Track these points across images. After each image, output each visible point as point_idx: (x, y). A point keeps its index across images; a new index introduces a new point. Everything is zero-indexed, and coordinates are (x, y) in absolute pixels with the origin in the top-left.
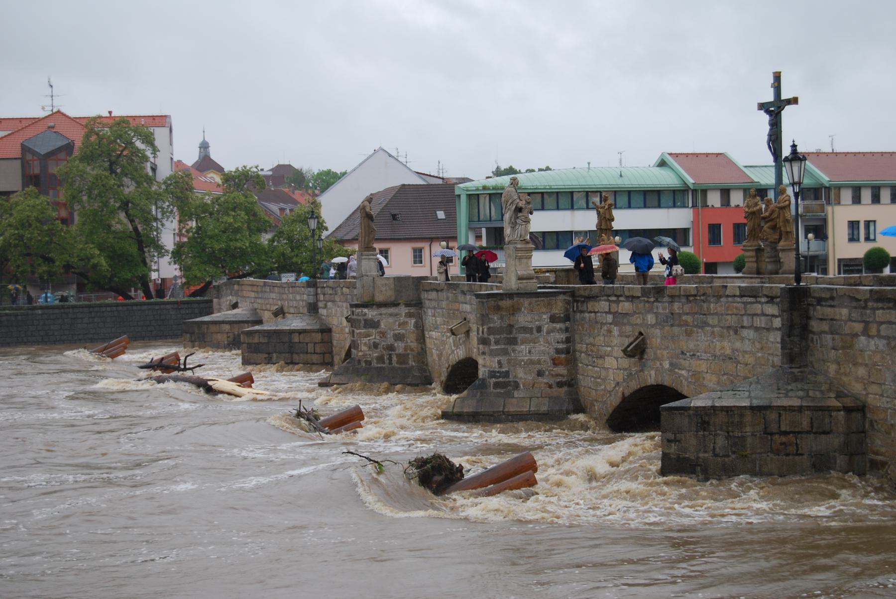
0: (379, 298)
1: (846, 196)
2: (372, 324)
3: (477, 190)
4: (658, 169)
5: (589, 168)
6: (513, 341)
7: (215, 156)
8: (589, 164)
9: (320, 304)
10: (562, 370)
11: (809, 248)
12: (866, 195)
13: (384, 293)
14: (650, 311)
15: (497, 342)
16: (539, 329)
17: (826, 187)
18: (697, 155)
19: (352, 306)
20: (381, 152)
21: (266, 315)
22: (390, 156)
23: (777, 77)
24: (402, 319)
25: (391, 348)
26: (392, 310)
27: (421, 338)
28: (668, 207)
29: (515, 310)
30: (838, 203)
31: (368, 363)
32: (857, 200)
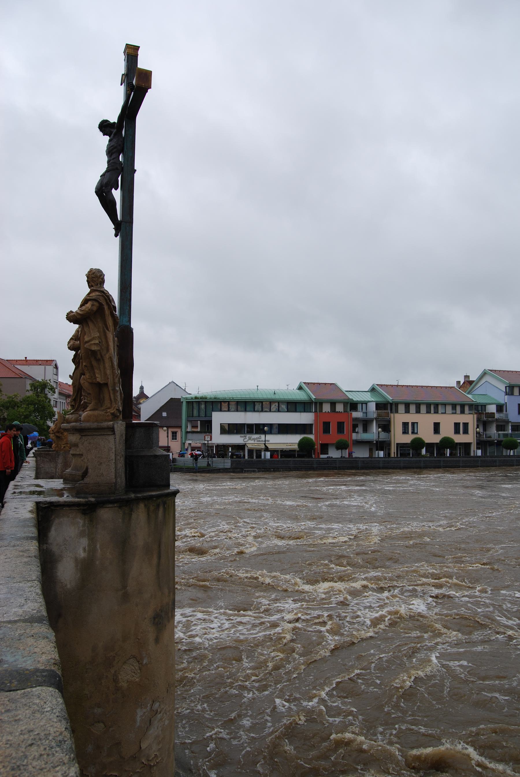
1: (401, 408)
3: (192, 399)
4: (298, 391)
5: (258, 389)
8: (258, 386)
11: (379, 437)
12: (413, 408)
17: (390, 403)
18: (320, 384)
20: (172, 384)
22: (177, 385)
28: (301, 412)
30: (397, 412)
32: (407, 411)
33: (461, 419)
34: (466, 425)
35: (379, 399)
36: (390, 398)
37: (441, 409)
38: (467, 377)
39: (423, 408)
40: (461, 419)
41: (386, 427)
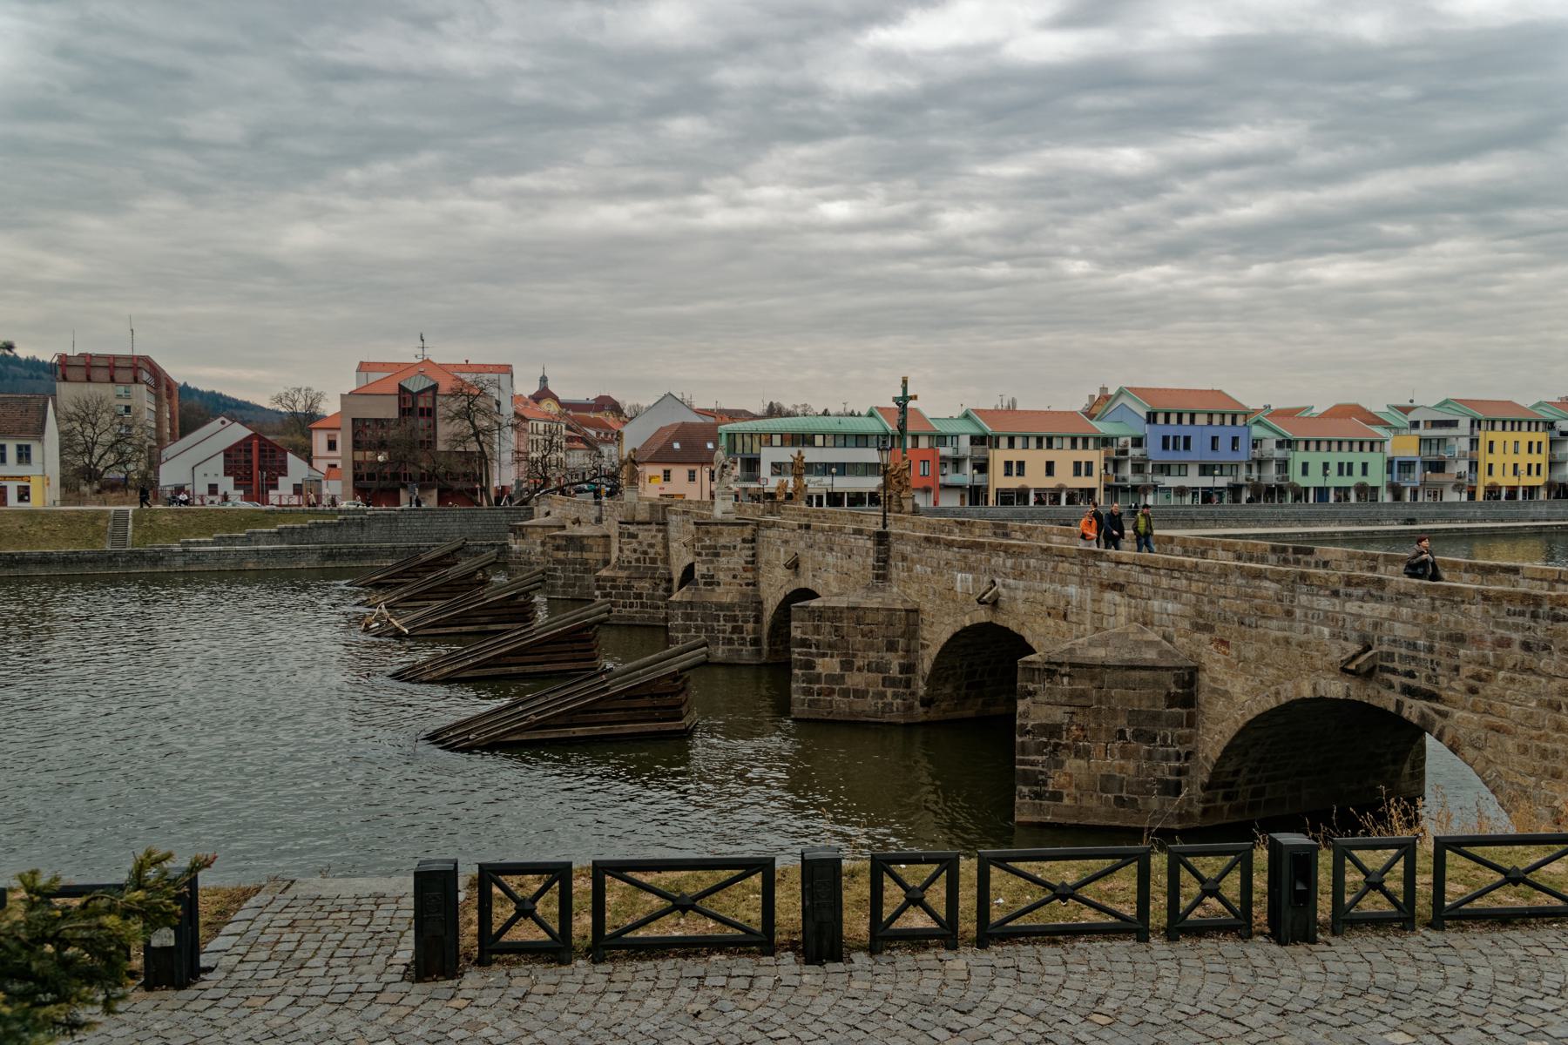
0: (639, 518)
1: (1004, 442)
2: (634, 536)
6: (717, 555)
7: (552, 387)
9: (604, 518)
10: (749, 575)
13: (642, 515)
14: (802, 538)
15: (707, 555)
16: (735, 547)
19: (621, 523)
21: (568, 524)
23: (905, 381)
24: (654, 533)
25: (645, 553)
26: (646, 527)
27: (666, 547)
29: (720, 533)
30: (997, 446)
31: (630, 562)
32: (1011, 444)
33: (1082, 455)
34: (1089, 464)
35: (976, 431)
36: (989, 430)
37: (1056, 443)
38: (1104, 389)
39: (1033, 442)
40: (1082, 455)
41: (982, 467)
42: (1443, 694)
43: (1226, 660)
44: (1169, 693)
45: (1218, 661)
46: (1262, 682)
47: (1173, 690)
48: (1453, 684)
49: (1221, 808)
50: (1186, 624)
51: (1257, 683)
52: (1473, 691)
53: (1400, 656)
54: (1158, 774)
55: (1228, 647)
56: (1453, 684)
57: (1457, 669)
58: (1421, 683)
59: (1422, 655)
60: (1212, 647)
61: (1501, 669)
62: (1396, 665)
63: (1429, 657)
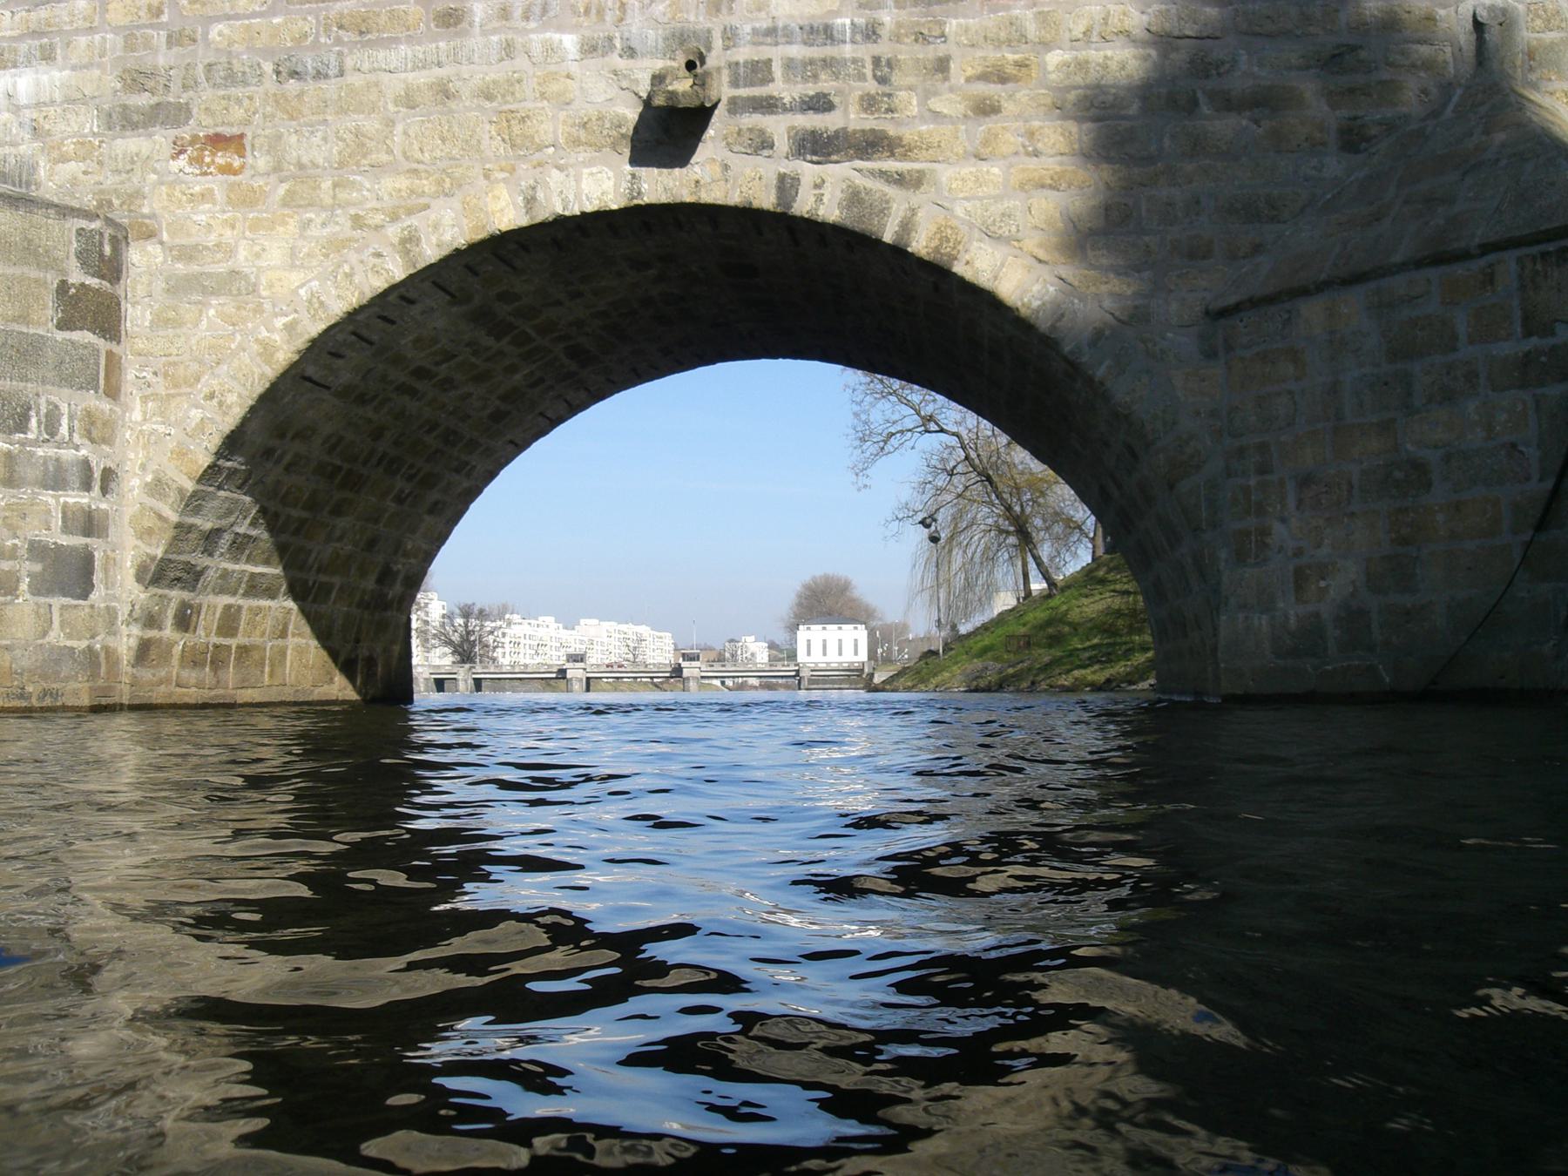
42: (908, 134)
43: (232, 187)
44: (63, 287)
45: (206, 196)
46: (357, 222)
47: (77, 277)
48: (936, 104)
49: (171, 645)
50: (88, 122)
51: (342, 226)
52: (986, 109)
53: (789, 64)
54: (33, 531)
55: (241, 152)
56: (936, 104)
57: (942, 66)
58: (848, 118)
59: (847, 51)
60: (182, 162)
61: (1047, 46)
62: (781, 88)
63: (865, 52)
